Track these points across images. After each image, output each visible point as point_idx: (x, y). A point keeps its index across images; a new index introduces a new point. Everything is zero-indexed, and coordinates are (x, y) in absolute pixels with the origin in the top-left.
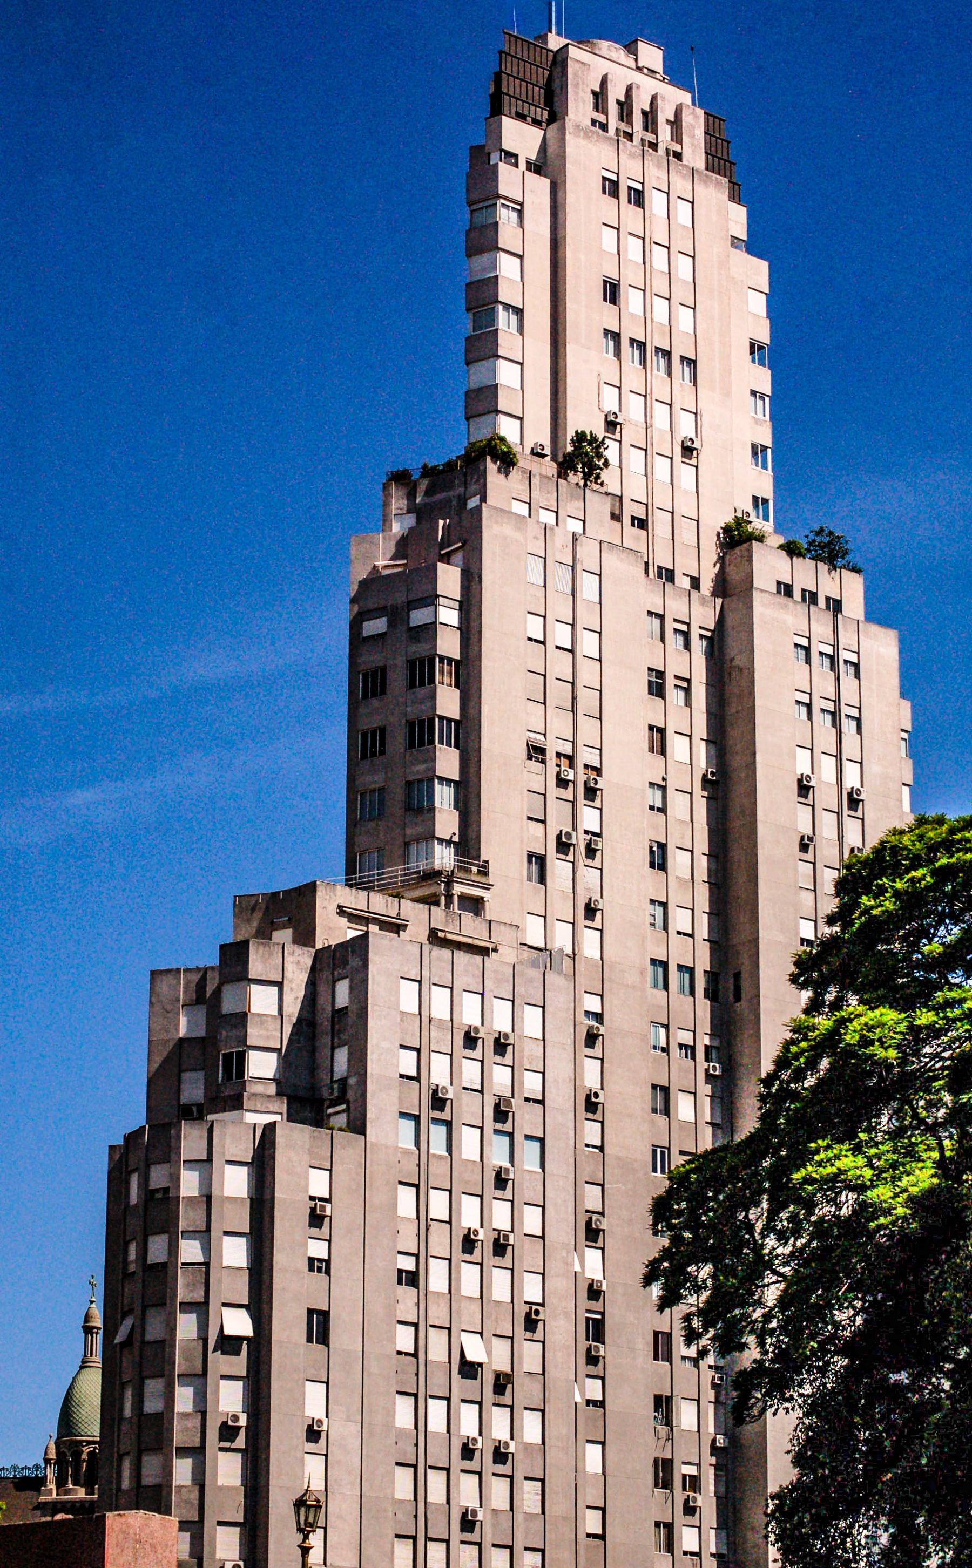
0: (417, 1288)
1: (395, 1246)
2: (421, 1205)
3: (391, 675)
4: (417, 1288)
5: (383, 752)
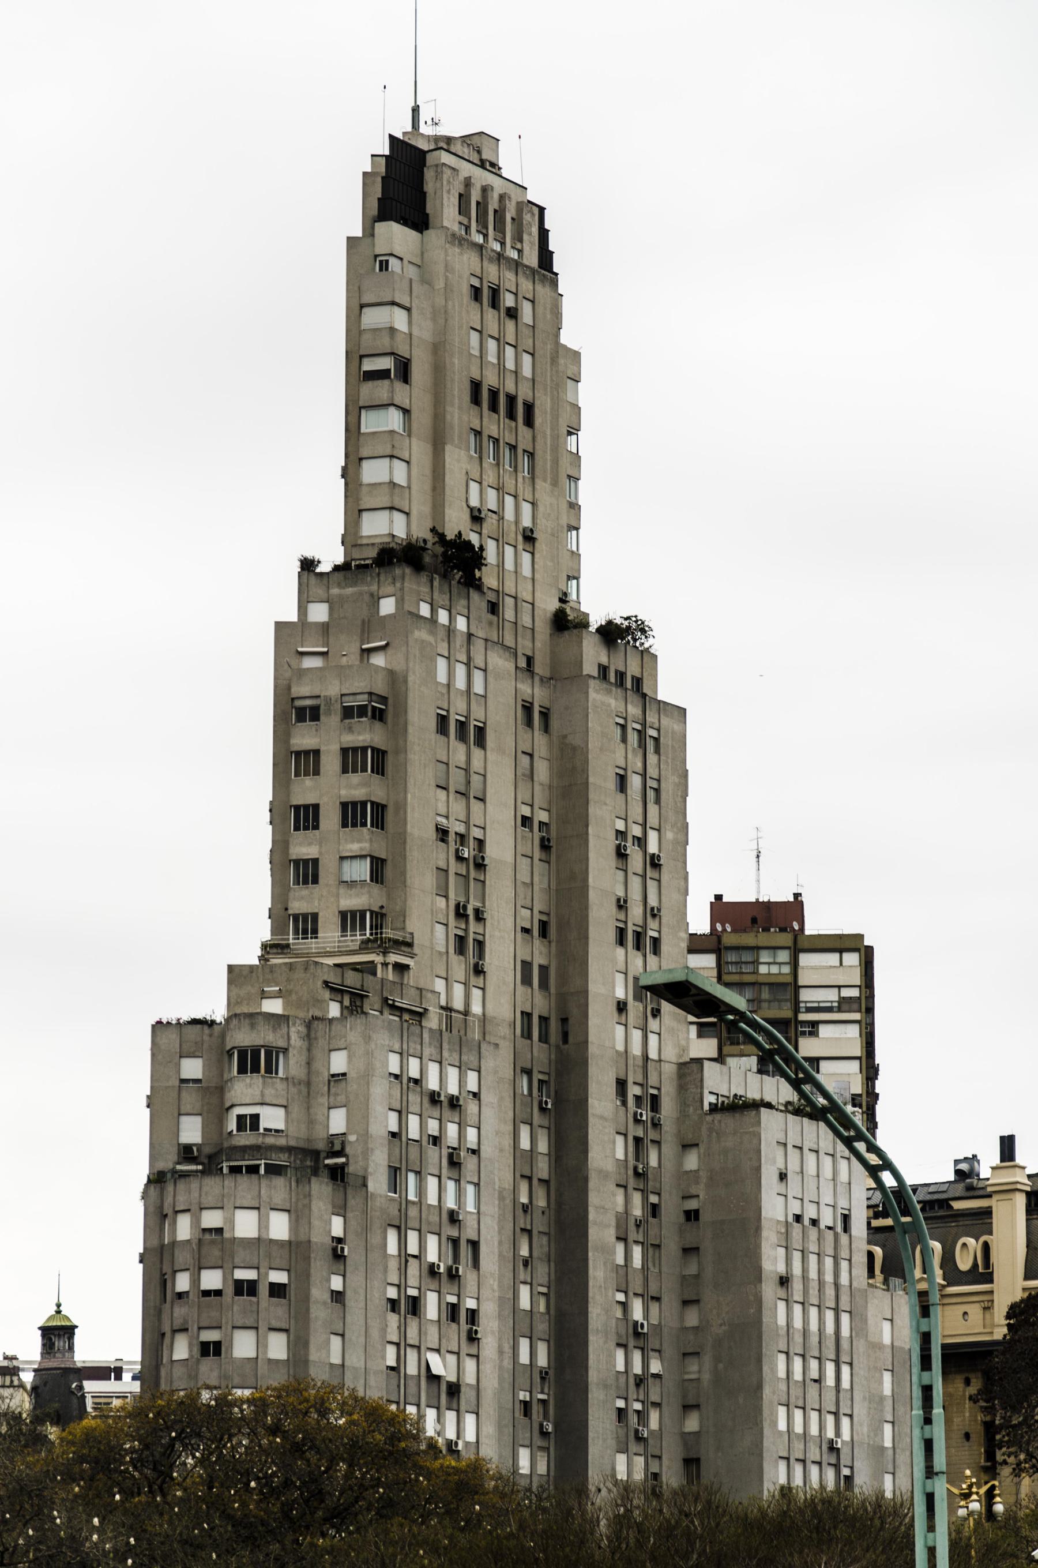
0: (399, 1314)
1: (386, 1279)
2: (402, 1242)
3: (324, 759)
4: (399, 1314)
5: (316, 827)
